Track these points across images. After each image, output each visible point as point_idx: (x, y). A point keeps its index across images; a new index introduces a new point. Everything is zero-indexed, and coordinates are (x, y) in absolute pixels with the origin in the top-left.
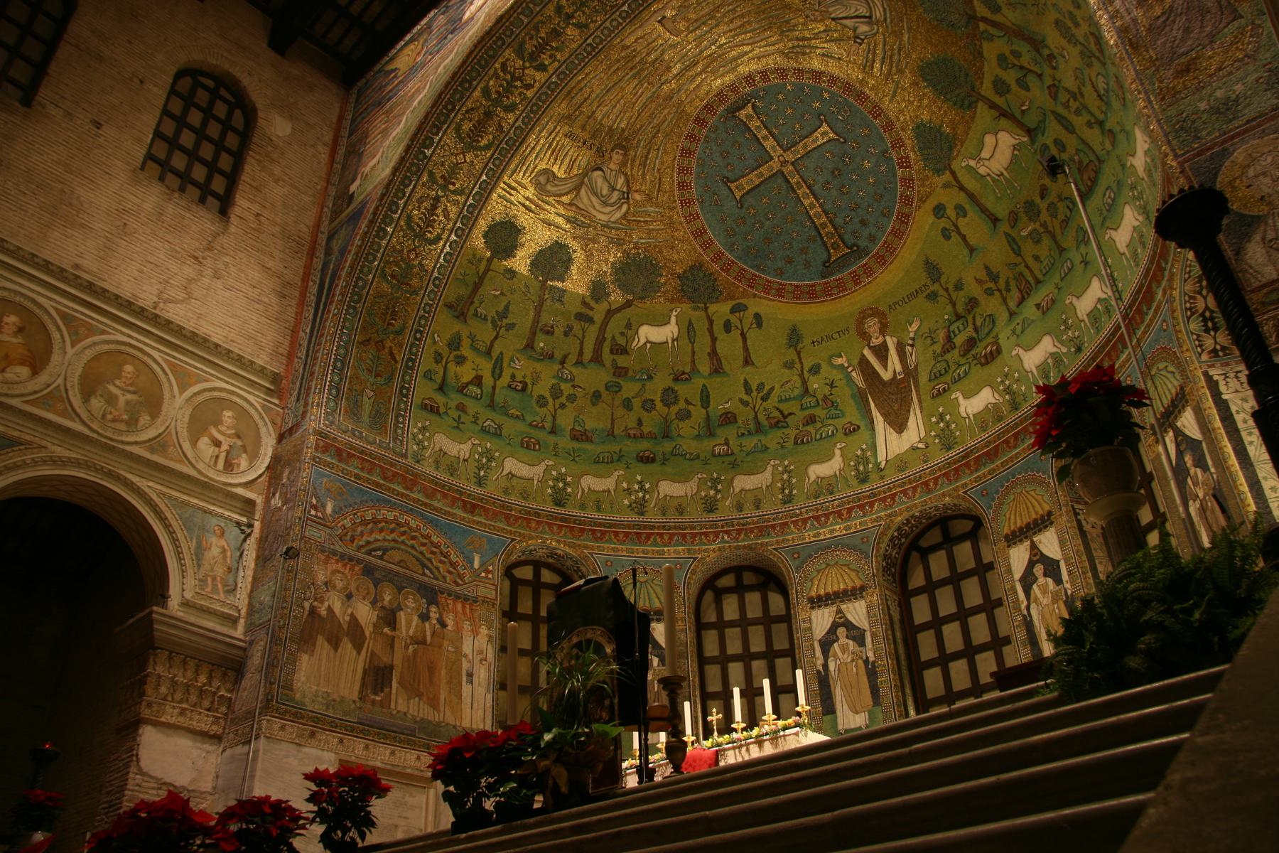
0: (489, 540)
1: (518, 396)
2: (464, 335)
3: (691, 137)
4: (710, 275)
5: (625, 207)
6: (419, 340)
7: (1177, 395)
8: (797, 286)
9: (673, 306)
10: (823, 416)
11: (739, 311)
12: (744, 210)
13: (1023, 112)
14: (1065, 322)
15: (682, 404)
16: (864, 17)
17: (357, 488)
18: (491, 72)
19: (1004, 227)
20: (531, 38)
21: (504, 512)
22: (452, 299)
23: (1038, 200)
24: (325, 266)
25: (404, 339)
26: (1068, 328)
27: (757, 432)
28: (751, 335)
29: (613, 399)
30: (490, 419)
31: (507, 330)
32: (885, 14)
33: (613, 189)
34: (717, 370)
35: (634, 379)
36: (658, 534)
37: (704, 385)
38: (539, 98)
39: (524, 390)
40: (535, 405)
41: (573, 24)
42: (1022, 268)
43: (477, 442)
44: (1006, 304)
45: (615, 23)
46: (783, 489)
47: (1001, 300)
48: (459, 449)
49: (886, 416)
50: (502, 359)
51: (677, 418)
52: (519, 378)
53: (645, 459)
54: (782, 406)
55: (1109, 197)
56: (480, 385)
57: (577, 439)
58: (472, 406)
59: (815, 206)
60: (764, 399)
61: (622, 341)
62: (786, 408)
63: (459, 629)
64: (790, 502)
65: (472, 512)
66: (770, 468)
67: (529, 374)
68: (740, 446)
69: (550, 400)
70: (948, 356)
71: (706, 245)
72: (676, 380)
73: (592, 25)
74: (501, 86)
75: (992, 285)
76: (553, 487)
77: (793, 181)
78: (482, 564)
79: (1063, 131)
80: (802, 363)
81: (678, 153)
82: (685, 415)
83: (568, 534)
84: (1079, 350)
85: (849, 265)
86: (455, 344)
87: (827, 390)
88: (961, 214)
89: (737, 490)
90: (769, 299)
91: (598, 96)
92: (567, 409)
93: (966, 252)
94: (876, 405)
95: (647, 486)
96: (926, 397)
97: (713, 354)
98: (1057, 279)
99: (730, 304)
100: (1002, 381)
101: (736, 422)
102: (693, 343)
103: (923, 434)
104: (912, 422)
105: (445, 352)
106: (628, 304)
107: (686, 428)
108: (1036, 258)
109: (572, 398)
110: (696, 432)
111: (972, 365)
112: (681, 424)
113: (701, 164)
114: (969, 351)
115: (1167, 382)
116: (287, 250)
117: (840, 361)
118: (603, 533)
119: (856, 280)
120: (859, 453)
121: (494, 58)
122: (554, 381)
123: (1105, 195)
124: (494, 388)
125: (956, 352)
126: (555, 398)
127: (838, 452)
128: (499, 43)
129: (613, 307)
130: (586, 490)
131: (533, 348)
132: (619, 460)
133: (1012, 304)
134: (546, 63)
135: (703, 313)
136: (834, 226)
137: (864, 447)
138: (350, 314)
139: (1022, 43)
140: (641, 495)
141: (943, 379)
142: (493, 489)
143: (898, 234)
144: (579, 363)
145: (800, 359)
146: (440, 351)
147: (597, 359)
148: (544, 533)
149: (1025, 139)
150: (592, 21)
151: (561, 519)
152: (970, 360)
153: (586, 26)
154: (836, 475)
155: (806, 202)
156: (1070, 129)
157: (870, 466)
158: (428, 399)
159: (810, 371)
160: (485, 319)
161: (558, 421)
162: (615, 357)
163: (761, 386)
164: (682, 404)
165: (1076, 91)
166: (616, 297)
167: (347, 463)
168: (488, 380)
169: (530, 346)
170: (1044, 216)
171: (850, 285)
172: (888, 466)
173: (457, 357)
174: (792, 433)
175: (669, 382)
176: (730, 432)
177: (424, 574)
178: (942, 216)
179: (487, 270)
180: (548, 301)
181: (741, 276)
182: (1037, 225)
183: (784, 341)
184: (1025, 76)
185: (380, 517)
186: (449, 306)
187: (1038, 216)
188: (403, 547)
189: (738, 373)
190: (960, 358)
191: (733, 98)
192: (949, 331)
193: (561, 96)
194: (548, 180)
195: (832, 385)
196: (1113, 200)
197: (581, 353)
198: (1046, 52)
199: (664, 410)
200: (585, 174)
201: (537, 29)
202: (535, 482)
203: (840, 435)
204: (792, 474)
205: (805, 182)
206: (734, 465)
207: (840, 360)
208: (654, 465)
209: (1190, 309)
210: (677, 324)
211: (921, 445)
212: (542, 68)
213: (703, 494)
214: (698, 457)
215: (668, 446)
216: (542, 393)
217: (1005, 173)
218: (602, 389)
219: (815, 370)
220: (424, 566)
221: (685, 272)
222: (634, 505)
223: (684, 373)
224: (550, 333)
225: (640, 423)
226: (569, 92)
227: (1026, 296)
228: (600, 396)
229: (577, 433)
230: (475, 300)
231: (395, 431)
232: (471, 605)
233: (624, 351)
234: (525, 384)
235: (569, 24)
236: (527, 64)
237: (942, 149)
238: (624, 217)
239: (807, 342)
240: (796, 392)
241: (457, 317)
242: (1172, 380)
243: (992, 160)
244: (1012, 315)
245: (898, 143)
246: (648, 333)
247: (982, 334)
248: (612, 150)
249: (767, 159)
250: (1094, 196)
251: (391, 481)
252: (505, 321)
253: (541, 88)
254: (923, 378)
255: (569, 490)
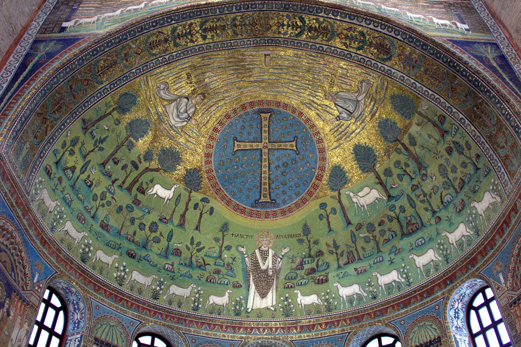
0: (46, 267)
1: (86, 188)
2: (81, 141)
3: (235, 111)
4: (201, 177)
5: (185, 123)
6: (62, 130)
7: (435, 339)
8: (238, 205)
9: (176, 182)
10: (224, 273)
11: (205, 202)
12: (234, 157)
13: (392, 187)
14: (369, 283)
15: (158, 234)
16: (349, 112)
17: (3, 202)
18: (184, 23)
19: (352, 228)
20: (212, 22)
21: (57, 252)
22: (87, 118)
23: (376, 225)
24: (28, 56)
25: (56, 124)
26: (370, 285)
27: (189, 266)
28: (205, 216)
29: (127, 214)
30: (70, 194)
31: (99, 150)
32: (359, 116)
33: (186, 111)
34: (181, 225)
35: (141, 209)
36: (126, 300)
37: (172, 230)
38: (191, 50)
39: (90, 186)
40: (91, 198)
41: (234, 31)
42: (353, 249)
43: (59, 204)
44: (338, 262)
45: (249, 42)
46: (195, 302)
47: (336, 258)
48: (51, 204)
49: (257, 286)
50: (89, 164)
51: (153, 240)
52: (91, 179)
53: (132, 256)
54: (206, 259)
55: (421, 242)
56: (73, 172)
57: (103, 228)
58: (65, 182)
59: (266, 173)
60: (198, 251)
61: (145, 186)
62: (208, 260)
63: (15, 320)
64: (197, 310)
65: (43, 246)
66: (190, 288)
67: (96, 179)
68: (179, 269)
69: (99, 199)
70: (298, 272)
71: (208, 162)
72: (160, 220)
73: (239, 36)
74: (182, 32)
75: (334, 250)
76: (83, 249)
77: (264, 157)
78: (38, 282)
79: (408, 205)
80: (223, 242)
81: (224, 114)
82: (157, 241)
83: (83, 281)
84: (374, 298)
85: (268, 208)
86: (74, 142)
87: (230, 261)
88: (333, 212)
89: (171, 292)
90: (221, 204)
91: (213, 67)
92: (104, 208)
93: (327, 229)
94: (253, 279)
95: (127, 270)
96: (281, 287)
97: (183, 216)
98: (371, 262)
99: (203, 196)
100: (324, 295)
101: (181, 256)
102: (176, 206)
103: (274, 303)
104: (270, 295)
105: (68, 144)
106: (157, 170)
107: (156, 248)
108: (363, 249)
109: (109, 203)
110: (159, 252)
111: (310, 281)
112: (154, 245)
113: (230, 126)
114: (310, 274)
115: (429, 332)
116: (7, 31)
117: (242, 249)
118: (100, 288)
119: (267, 216)
120: (238, 299)
121: (191, 18)
122: (105, 190)
123: (418, 239)
124: (78, 177)
125: (303, 271)
126: (102, 199)
127: (227, 294)
128: (199, 13)
129: (150, 167)
130: (98, 259)
131: (104, 167)
132: (118, 249)
133: (341, 263)
134: (208, 37)
135: (188, 193)
136: (269, 186)
137: (242, 297)
138: (41, 93)
139: (414, 162)
140: (123, 274)
141: (292, 281)
142: (56, 236)
143: (298, 206)
144: (120, 186)
145: (223, 239)
146: (67, 142)
147: (129, 189)
148: (72, 275)
149: (385, 198)
150: (241, 35)
151: (82, 270)
152: (310, 278)
153: (237, 34)
154: (223, 305)
155: (264, 169)
156: (413, 205)
157: (243, 308)
158: (50, 166)
159: (226, 247)
160: (93, 138)
161: (98, 212)
162: (138, 193)
163: (199, 244)
164: (158, 234)
165: (428, 193)
166: (154, 164)
167: (5, 183)
168: (77, 171)
169: (104, 164)
170: (377, 233)
171: (263, 216)
172: (252, 312)
173: (72, 150)
174: (207, 275)
175: (156, 220)
176: (176, 260)
177: (11, 275)
178: (323, 209)
179: (110, 113)
180: (124, 147)
181: (214, 186)
182: (370, 235)
183: (219, 226)
184: (404, 175)
185: (6, 227)
186: (84, 121)
187: (373, 231)
188: (9, 252)
189: (190, 231)
190: (305, 275)
191: (265, 106)
192: (303, 260)
193: (200, 55)
194: (164, 89)
195: (234, 259)
196: (422, 244)
197: (124, 182)
198: (424, 172)
199: (148, 233)
200: (180, 97)
201: (218, 20)
202: (76, 242)
203: (230, 286)
204: (201, 296)
205: (269, 161)
206: (173, 278)
207: (242, 249)
208: (133, 260)
209: (453, 305)
210: (174, 192)
211: (272, 308)
212: (204, 38)
213: (154, 287)
214: (156, 266)
215: (143, 253)
216: (97, 193)
217: (366, 207)
218: (124, 207)
219: (228, 248)
220: (13, 270)
221: (191, 169)
222: (118, 278)
223: (165, 219)
224: (116, 163)
225: (135, 234)
226: (205, 56)
227: (350, 262)
228: (122, 210)
229: (104, 225)
230: (96, 125)
231: (29, 177)
232: (25, 306)
233: (143, 192)
234: (92, 184)
235: (232, 28)
236: (200, 32)
237: (341, 181)
238: (183, 127)
239: (230, 233)
240: (215, 255)
241: (83, 129)
242: (434, 332)
243: (362, 198)
244: (339, 267)
245: (322, 169)
246: (158, 190)
247: (320, 269)
248: (199, 94)
249: (260, 141)
250: (411, 237)
251: (18, 206)
252: (101, 145)
253: (196, 46)
254: (282, 277)
255: (90, 255)
